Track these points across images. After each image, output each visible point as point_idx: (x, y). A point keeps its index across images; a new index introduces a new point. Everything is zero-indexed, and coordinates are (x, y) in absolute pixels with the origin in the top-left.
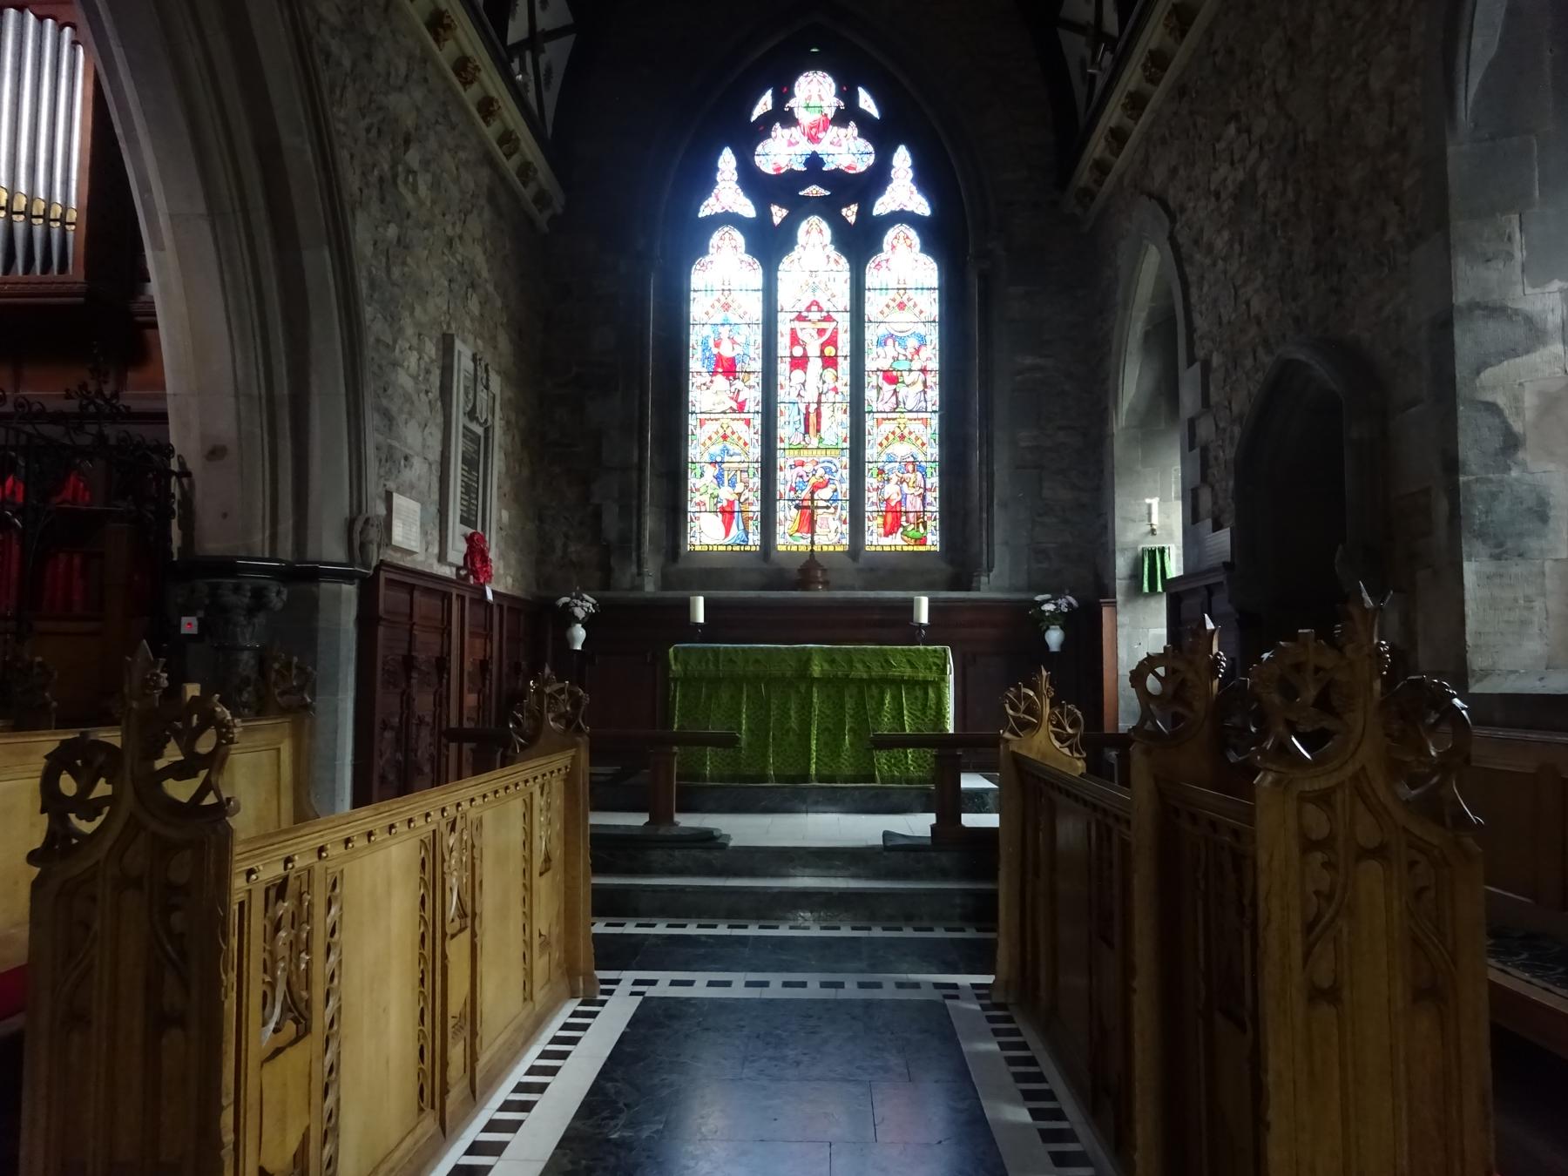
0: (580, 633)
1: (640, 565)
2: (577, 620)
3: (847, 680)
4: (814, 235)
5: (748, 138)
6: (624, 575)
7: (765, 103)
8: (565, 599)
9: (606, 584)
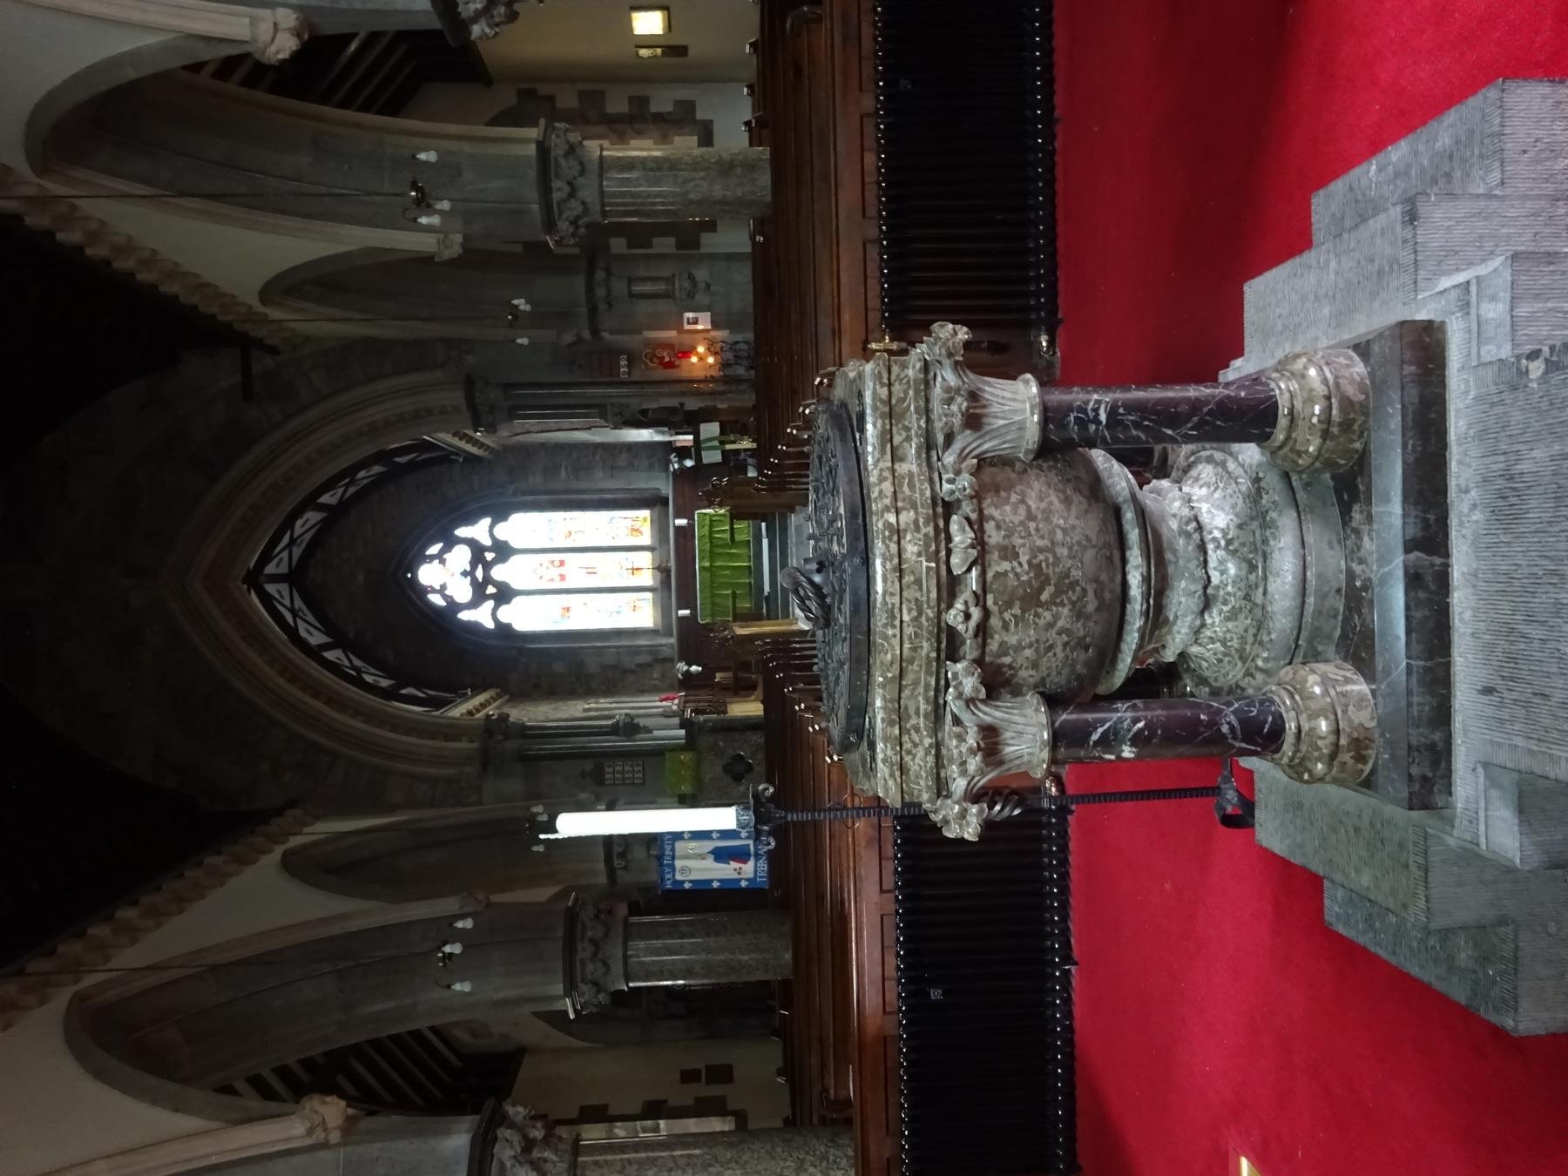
0: (694, 668)
1: (662, 645)
2: (688, 671)
3: (711, 551)
4: (499, 573)
5: (454, 607)
6: (667, 652)
7: (436, 599)
8: (680, 675)
9: (671, 660)
